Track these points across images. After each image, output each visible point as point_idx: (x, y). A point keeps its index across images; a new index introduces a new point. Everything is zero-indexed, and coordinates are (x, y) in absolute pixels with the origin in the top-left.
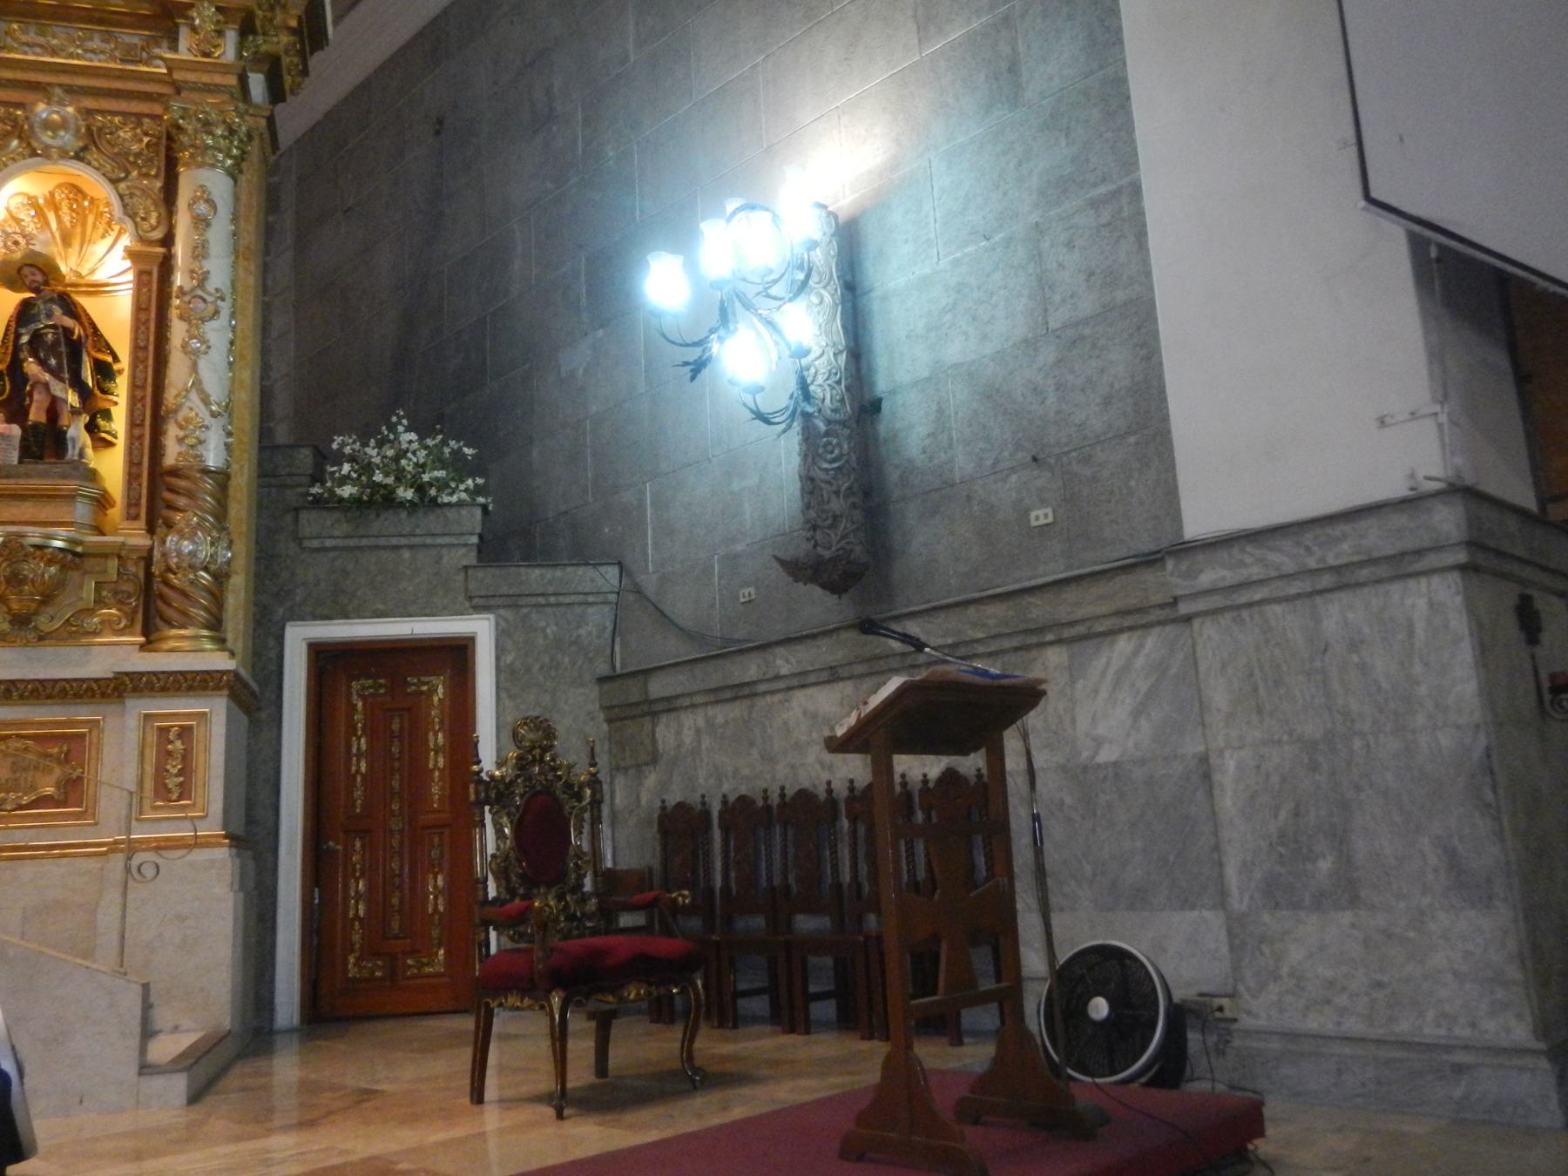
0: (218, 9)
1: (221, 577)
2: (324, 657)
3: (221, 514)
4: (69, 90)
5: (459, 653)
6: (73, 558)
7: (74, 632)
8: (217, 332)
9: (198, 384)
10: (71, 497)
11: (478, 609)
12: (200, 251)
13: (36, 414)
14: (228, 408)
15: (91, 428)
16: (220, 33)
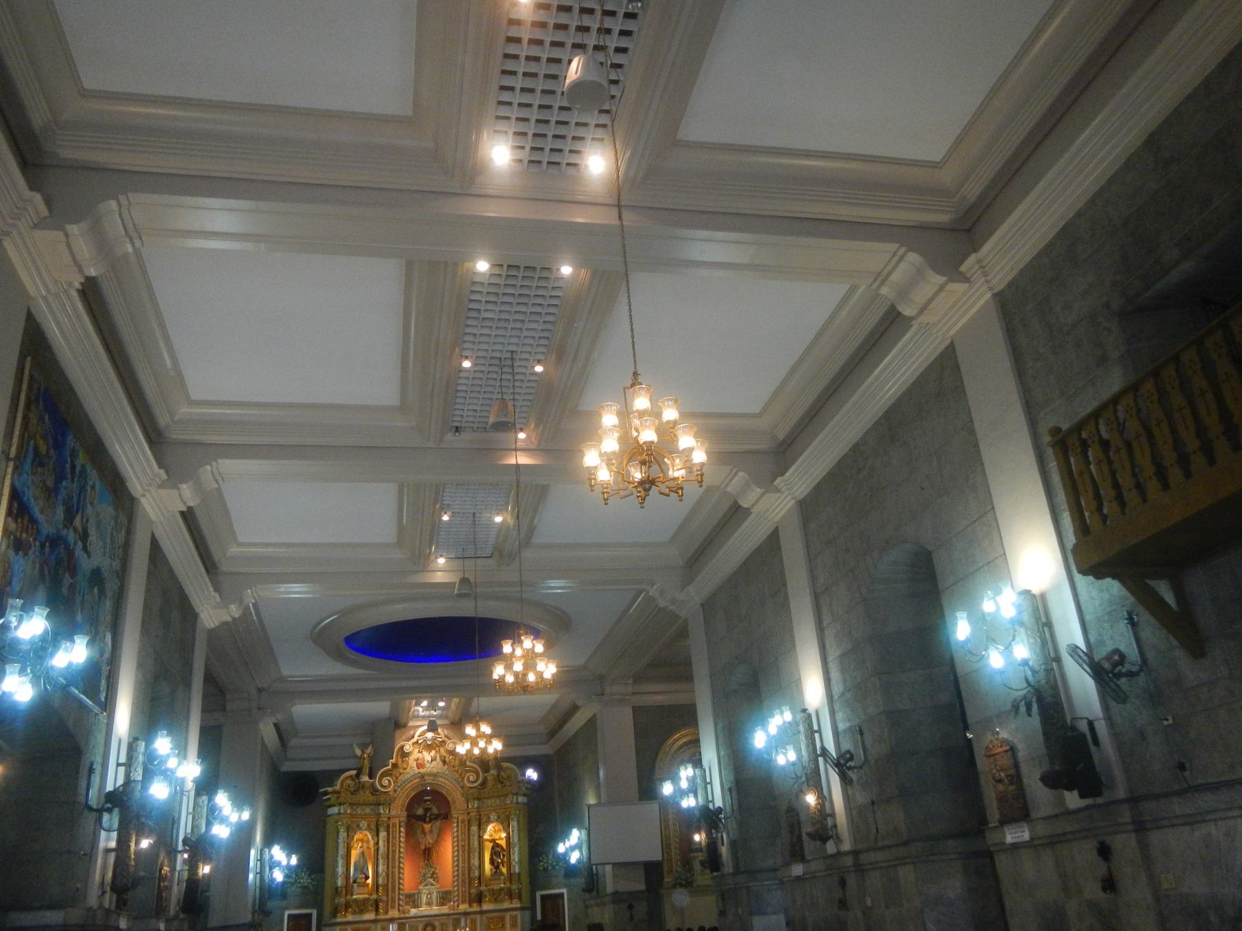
0: (513, 794)
1: (520, 890)
2: (543, 898)
3: (519, 878)
4: (495, 810)
6: (501, 889)
7: (502, 901)
8: (516, 849)
9: (514, 860)
10: (499, 879)
11: (566, 886)
12: (513, 837)
13: (496, 864)
14: (520, 861)
15: (503, 865)
16: (513, 798)
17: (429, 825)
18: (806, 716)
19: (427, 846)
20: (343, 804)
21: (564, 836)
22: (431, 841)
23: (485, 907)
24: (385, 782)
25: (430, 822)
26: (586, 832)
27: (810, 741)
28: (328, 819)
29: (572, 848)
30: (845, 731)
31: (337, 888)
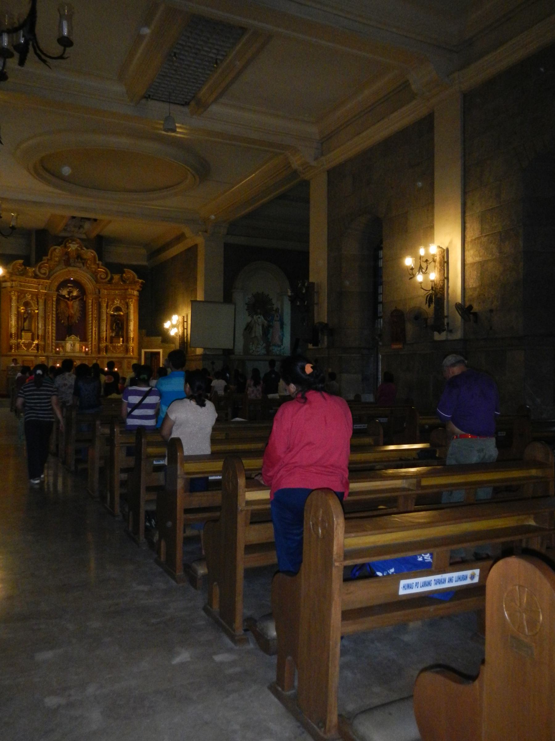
2: (145, 353)
5: (159, 353)
11: (160, 348)
14: (134, 331)
17: (72, 302)
18: (443, 251)
19: (70, 315)
20: (16, 281)
21: (170, 319)
22: (72, 312)
23: (109, 355)
24: (43, 271)
25: (72, 300)
26: (182, 317)
27: (443, 268)
28: (3, 290)
29: (173, 326)
30: (473, 264)
31: (11, 334)
